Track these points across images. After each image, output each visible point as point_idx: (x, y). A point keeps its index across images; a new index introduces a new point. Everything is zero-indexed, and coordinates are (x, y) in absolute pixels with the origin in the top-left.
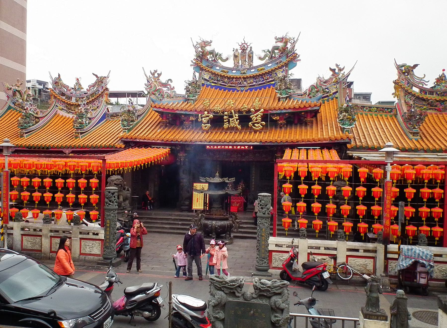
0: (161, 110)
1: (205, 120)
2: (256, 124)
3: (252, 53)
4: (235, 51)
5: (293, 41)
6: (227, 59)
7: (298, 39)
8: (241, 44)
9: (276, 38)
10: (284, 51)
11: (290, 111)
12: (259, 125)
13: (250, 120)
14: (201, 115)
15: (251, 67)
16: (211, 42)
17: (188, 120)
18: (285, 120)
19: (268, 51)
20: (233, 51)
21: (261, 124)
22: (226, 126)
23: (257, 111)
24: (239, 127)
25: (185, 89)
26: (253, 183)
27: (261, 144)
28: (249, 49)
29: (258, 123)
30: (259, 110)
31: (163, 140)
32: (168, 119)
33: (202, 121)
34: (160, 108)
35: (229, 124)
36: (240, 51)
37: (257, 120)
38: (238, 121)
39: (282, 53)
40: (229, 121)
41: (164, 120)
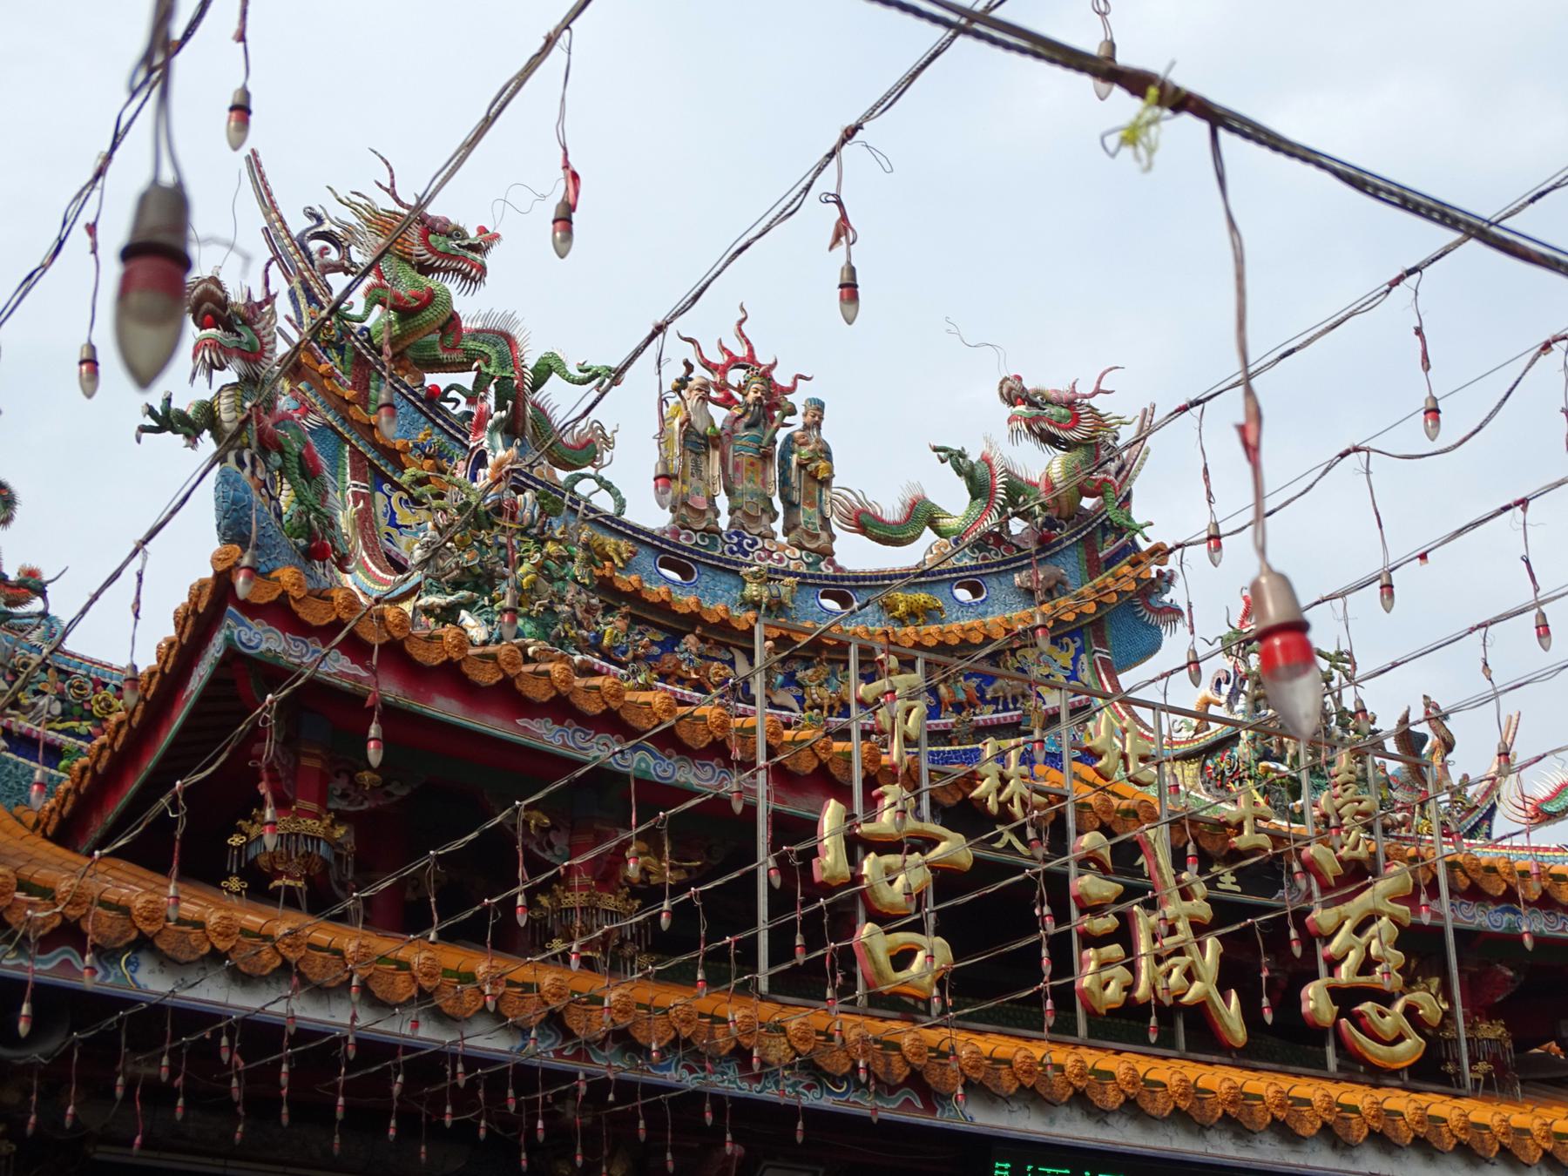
3: (826, 453)
40: (1124, 934)
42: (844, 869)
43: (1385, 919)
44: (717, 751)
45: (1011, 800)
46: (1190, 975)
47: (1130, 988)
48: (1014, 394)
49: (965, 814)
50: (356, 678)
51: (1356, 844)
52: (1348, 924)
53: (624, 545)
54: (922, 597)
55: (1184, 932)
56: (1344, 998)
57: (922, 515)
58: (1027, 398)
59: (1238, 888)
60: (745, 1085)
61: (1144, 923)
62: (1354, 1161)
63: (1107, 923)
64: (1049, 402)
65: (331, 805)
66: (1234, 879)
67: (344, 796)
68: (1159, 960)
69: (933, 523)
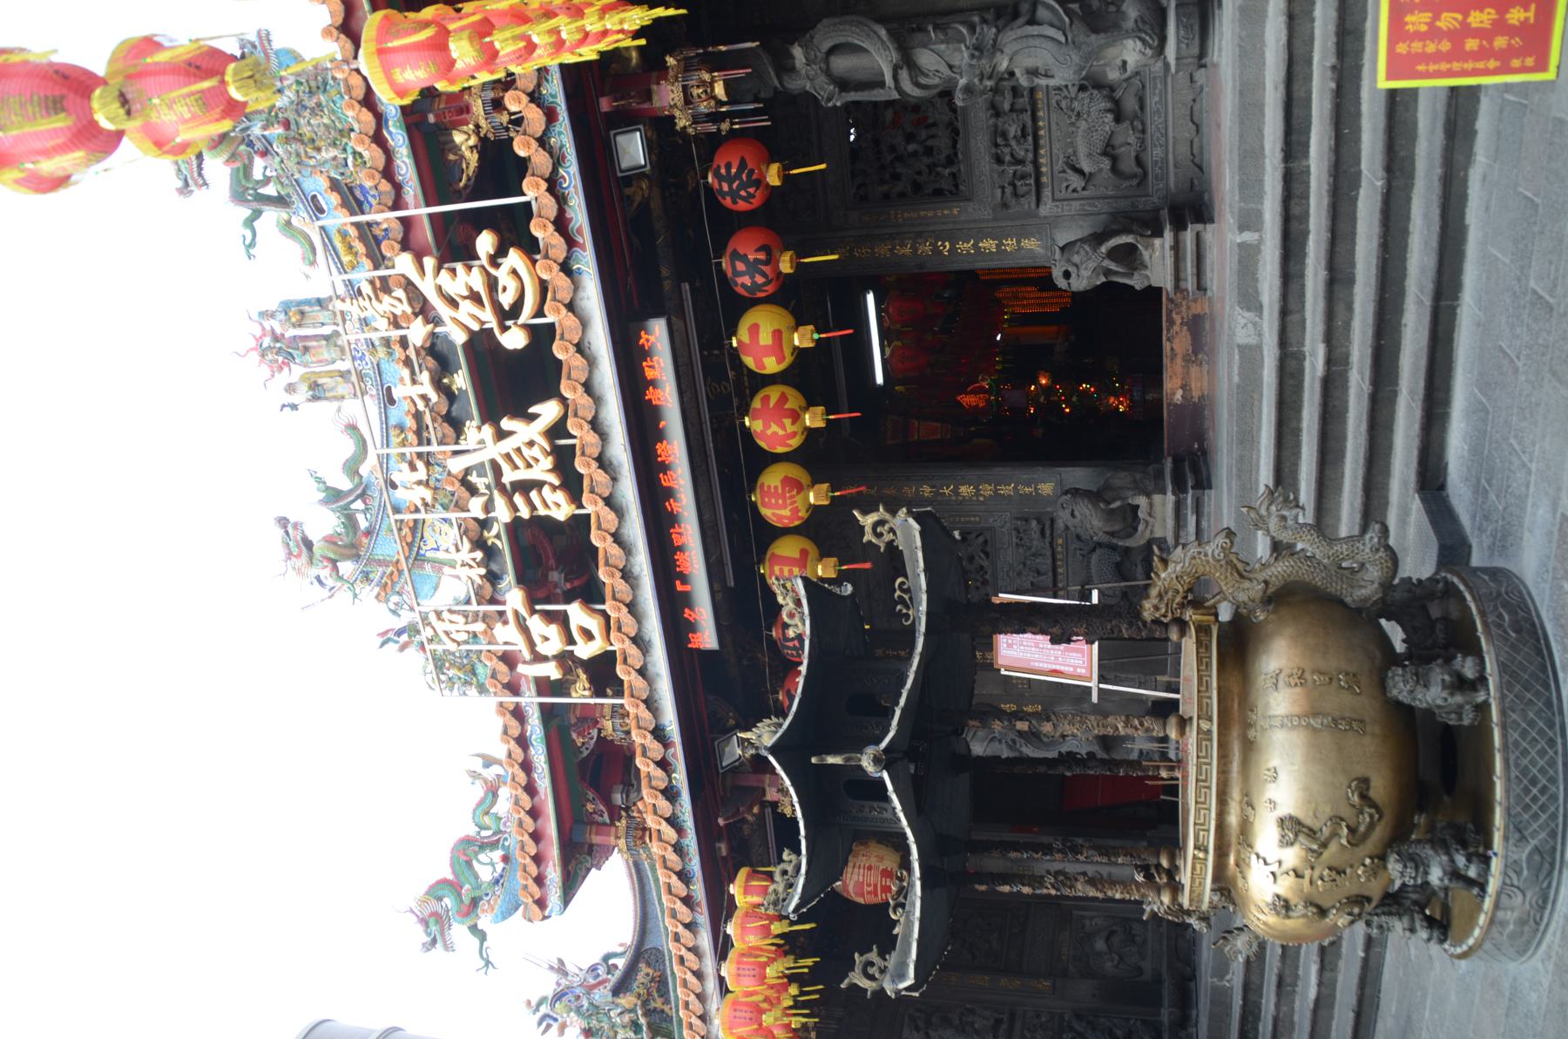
0: (554, 874)
1: (550, 640)
3: (286, 307)
4: (294, 399)
6: (352, 428)
9: (185, 189)
12: (502, 275)
13: (481, 346)
14: (525, 662)
16: (283, 522)
17: (588, 717)
19: (249, 223)
20: (294, 407)
21: (494, 260)
22: (559, 508)
24: (548, 411)
26: (989, 245)
27: (587, 262)
29: (492, 284)
30: (409, 286)
31: (691, 926)
32: (614, 813)
33: (564, 659)
34: (540, 880)
35: (539, 485)
36: (297, 372)
37: (475, 297)
39: (251, 144)
40: (525, 487)
42: (553, 664)
46: (531, 444)
47: (554, 488)
48: (185, 189)
53: (393, 433)
54: (339, 245)
55: (507, 445)
58: (187, 184)
61: (509, 476)
62: (620, 465)
63: (518, 499)
68: (529, 466)
69: (288, 223)
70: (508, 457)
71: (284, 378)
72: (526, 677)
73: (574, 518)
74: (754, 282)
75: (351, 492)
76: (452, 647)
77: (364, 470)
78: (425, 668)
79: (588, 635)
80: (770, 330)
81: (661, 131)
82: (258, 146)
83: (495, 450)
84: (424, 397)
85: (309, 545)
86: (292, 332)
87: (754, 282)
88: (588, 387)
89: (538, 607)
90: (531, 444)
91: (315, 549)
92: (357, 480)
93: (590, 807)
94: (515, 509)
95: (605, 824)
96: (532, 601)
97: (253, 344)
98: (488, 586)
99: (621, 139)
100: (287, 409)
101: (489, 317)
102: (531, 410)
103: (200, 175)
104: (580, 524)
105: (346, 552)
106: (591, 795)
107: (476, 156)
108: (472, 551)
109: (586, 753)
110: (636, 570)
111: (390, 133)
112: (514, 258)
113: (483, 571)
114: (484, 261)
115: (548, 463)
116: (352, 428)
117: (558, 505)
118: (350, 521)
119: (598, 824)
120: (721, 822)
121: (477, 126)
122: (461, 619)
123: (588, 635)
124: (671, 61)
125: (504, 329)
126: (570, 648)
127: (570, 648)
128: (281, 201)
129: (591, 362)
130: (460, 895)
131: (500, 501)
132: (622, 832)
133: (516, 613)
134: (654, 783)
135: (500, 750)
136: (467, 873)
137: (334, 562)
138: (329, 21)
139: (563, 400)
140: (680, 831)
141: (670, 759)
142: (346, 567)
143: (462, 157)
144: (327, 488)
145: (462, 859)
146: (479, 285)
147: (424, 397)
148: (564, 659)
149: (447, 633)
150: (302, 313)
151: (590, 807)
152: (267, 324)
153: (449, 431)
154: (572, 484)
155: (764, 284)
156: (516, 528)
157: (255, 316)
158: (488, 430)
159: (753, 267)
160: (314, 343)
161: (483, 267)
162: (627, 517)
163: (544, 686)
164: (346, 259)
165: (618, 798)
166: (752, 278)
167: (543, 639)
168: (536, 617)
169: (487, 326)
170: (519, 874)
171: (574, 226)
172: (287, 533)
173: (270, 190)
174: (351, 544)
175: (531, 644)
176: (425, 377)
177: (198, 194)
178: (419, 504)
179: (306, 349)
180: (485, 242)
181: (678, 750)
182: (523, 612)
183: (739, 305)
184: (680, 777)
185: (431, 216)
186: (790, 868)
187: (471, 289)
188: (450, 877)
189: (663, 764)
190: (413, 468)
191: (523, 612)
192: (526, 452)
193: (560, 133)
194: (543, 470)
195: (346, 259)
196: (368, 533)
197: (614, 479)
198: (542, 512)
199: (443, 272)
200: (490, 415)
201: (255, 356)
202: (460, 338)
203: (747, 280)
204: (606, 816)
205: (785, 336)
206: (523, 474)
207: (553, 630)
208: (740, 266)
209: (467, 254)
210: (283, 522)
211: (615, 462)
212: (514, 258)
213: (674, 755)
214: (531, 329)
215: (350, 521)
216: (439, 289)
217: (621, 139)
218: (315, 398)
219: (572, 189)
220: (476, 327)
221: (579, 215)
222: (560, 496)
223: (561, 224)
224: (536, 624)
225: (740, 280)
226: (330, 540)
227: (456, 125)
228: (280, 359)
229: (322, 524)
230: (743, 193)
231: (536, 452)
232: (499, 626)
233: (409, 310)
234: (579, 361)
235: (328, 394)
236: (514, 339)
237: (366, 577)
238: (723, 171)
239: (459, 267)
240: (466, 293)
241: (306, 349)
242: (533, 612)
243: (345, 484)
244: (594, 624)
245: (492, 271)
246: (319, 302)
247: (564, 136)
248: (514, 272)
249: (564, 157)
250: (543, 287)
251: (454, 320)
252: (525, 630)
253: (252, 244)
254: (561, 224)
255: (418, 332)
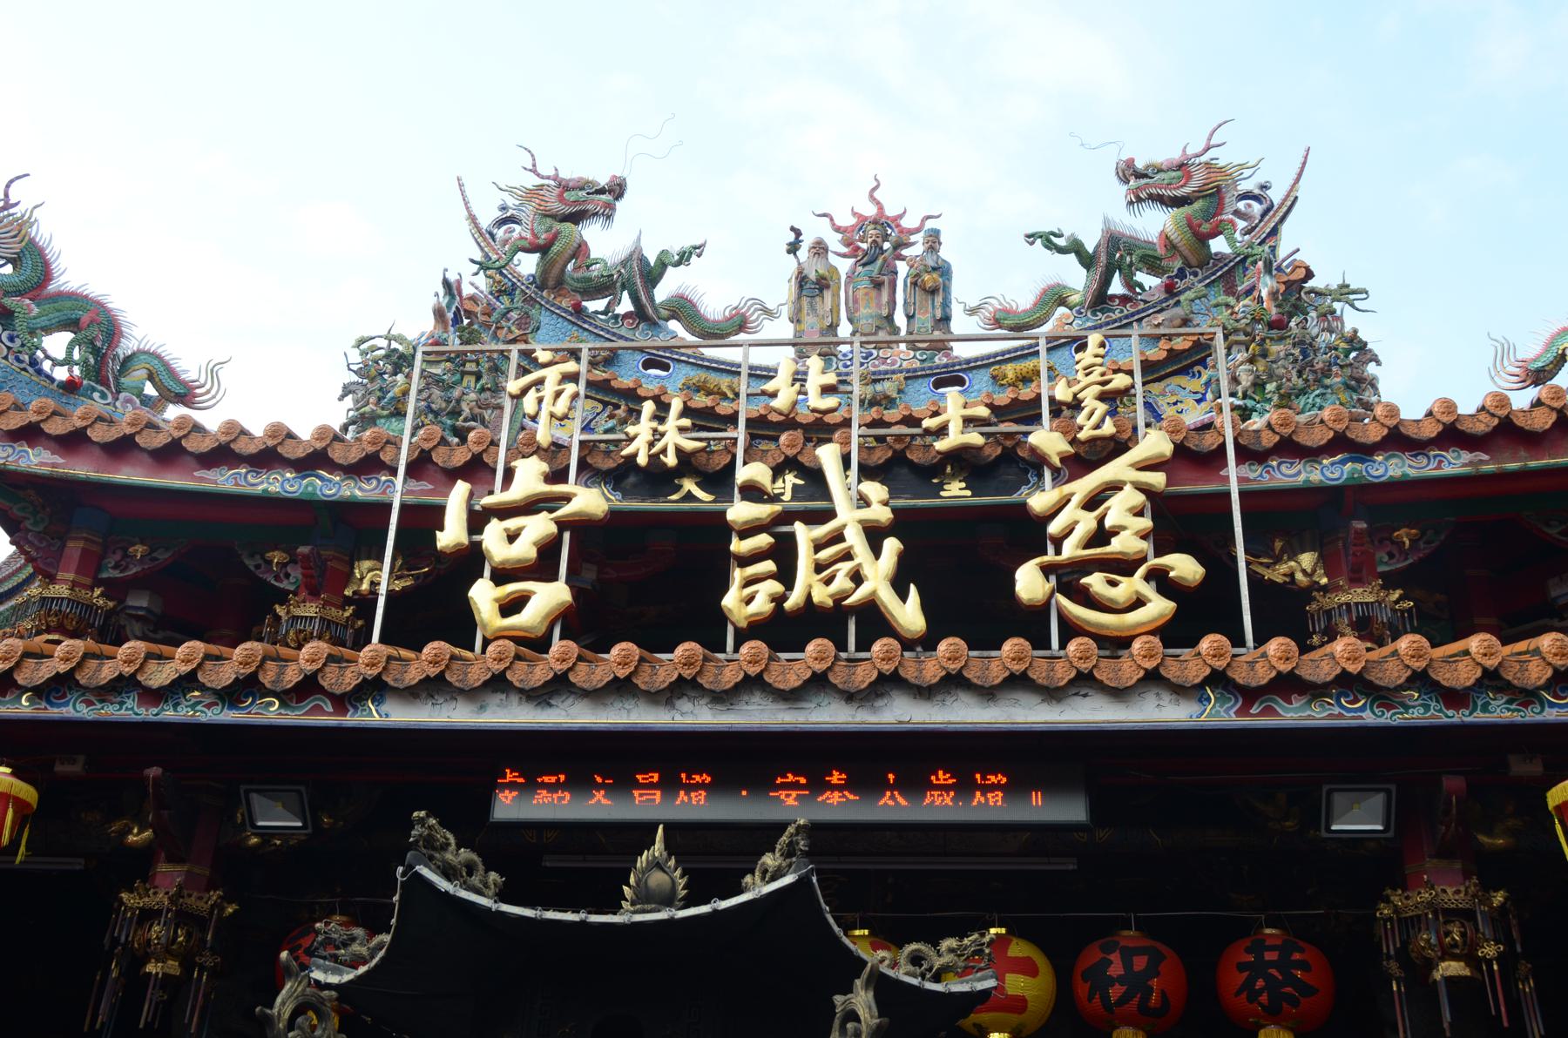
2: (1096, 582)
3: (943, 270)
4: (803, 253)
5: (1257, 208)
7: (1291, 203)
8: (850, 221)
9: (1128, 172)
10: (1189, 260)
11: (1455, 463)
14: (471, 494)
15: (940, 360)
16: (617, 189)
17: (327, 580)
18: (1389, 582)
19: (1076, 248)
20: (793, 248)
21: (1162, 581)
22: (746, 598)
23: (1086, 457)
24: (909, 614)
25: (347, 390)
27: (1218, 714)
28: (916, 250)
29: (1123, 566)
30: (1116, 447)
32: (114, 589)
33: (470, 561)
35: (786, 575)
37: (1101, 536)
38: (892, 546)
39: (1181, 274)
40: (784, 554)
41: (61, 590)
42: (464, 538)
43: (1128, 488)
44: (370, 465)
45: (664, 451)
47: (779, 600)
48: (1128, 172)
49: (621, 475)
50: (54, 465)
51: (1093, 421)
52: (1075, 500)
55: (855, 539)
56: (1068, 578)
57: (1056, 297)
58: (1139, 175)
59: (968, 493)
60: (142, 711)
61: (804, 535)
62: (875, 710)
63: (763, 540)
64: (1160, 171)
65: (104, 575)
66: (963, 485)
67: (115, 567)
68: (819, 568)
69: (1062, 302)
70: (838, 537)
71: (834, 242)
72: (447, 495)
73: (722, 618)
74: (1111, 981)
75: (652, 299)
76: (513, 386)
77: (674, 325)
78: (400, 339)
79: (511, 606)
80: (1028, 994)
81: (1379, 865)
82: (1180, 285)
83: (847, 517)
84: (942, 431)
85: (577, 218)
86: (902, 268)
87: (1111, 981)
88: (753, 684)
89: (567, 536)
90: (857, 578)
91: (568, 227)
92: (664, 313)
93: (139, 550)
94: (748, 531)
95: (99, 569)
96: (579, 527)
97: (890, 211)
98: (609, 464)
99: (1378, 800)
100: (791, 237)
101: (1070, 549)
102: (912, 588)
103: (1152, 197)
104: (710, 627)
105: (555, 271)
106: (163, 556)
107: (1280, 579)
108: (679, 451)
109: (250, 563)
110: (685, 705)
111: (1343, 462)
112: (1159, 607)
113: (642, 460)
114: (1154, 562)
115: (822, 595)
116: (738, 323)
117: (749, 600)
118: (605, 287)
119: (102, 557)
120: (154, 772)
121: (1325, 589)
122: (561, 406)
123: (511, 606)
124: (1499, 898)
125: (1047, 570)
126: (487, 573)
127: (487, 573)
128: (1100, 300)
129: (791, 697)
130: (20, 293)
131: (762, 511)
132: (83, 594)
133: (567, 498)
134: (270, 665)
135: (211, 420)
136: (55, 317)
137: (543, 249)
138: (1405, 415)
139: (928, 642)
140: (155, 696)
141: (309, 704)
142: (528, 264)
143: (1278, 560)
144: (662, 265)
145: (85, 318)
146: (1117, 545)
147: (942, 431)
148: (470, 561)
149: (540, 382)
150: (933, 292)
151: (139, 550)
152: (918, 238)
153: (881, 456)
154: (785, 629)
155: (1105, 998)
156: (719, 528)
157: (930, 224)
158: (882, 514)
159: (1136, 983)
160: (885, 297)
161: (1144, 560)
162: (782, 706)
163: (424, 519)
164: (1010, 370)
165: (139, 601)
166: (1121, 980)
167: (514, 530)
168: (553, 529)
169: (1051, 549)
170: (51, 404)
171: (1280, 706)
172: (601, 191)
173: (1117, 287)
174: (565, 281)
175: (505, 512)
176: (975, 438)
177: (1121, 191)
178: (769, 386)
179: (878, 285)
180: (1185, 567)
181: (328, 719)
182: (565, 510)
183: (1062, 950)
184: (272, 713)
185: (1228, 495)
186: (475, 880)
187: (1115, 532)
188: (52, 287)
189: (308, 687)
190: (827, 390)
191: (565, 510)
192: (845, 567)
193: (1427, 708)
194: (808, 586)
195: (1010, 370)
196: (579, 310)
197: (850, 697)
198: (738, 575)
199: (1141, 498)
200: (902, 524)
201: (870, 211)
202: (1039, 501)
203: (1116, 970)
204: (116, 574)
205: (1014, 1018)
206: (805, 559)
207: (525, 550)
208: (1140, 963)
209: (1163, 539)
210: (617, 189)
211: (880, 703)
212: (1159, 607)
213: (317, 710)
214: (1041, 611)
215: (605, 287)
216: (1116, 487)
217: (1378, 800)
218: (802, 280)
219: (1337, 710)
220: (1054, 528)
221: (1294, 714)
222: (762, 605)
223: (1288, 685)
224: (539, 527)
225: (1115, 957)
226: (580, 250)
227: (1328, 562)
228: (864, 246)
229: (605, 243)
230: (1260, 983)
231: (842, 582)
232: (544, 467)
233: (1082, 436)
234: (996, 674)
235: (805, 302)
236: (1029, 582)
237: (504, 290)
238: (1297, 956)
239: (1146, 523)
240: (1108, 523)
241: (878, 285)
242: (562, 525)
243: (662, 293)
244: (530, 617)
245: (1142, 571)
246: (946, 319)
247: (1419, 713)
248: (1139, 602)
249: (1389, 707)
250: (1116, 644)
251: (1066, 501)
252: (530, 507)
253: (1050, 245)
254: (1288, 685)
255: (1047, 439)
